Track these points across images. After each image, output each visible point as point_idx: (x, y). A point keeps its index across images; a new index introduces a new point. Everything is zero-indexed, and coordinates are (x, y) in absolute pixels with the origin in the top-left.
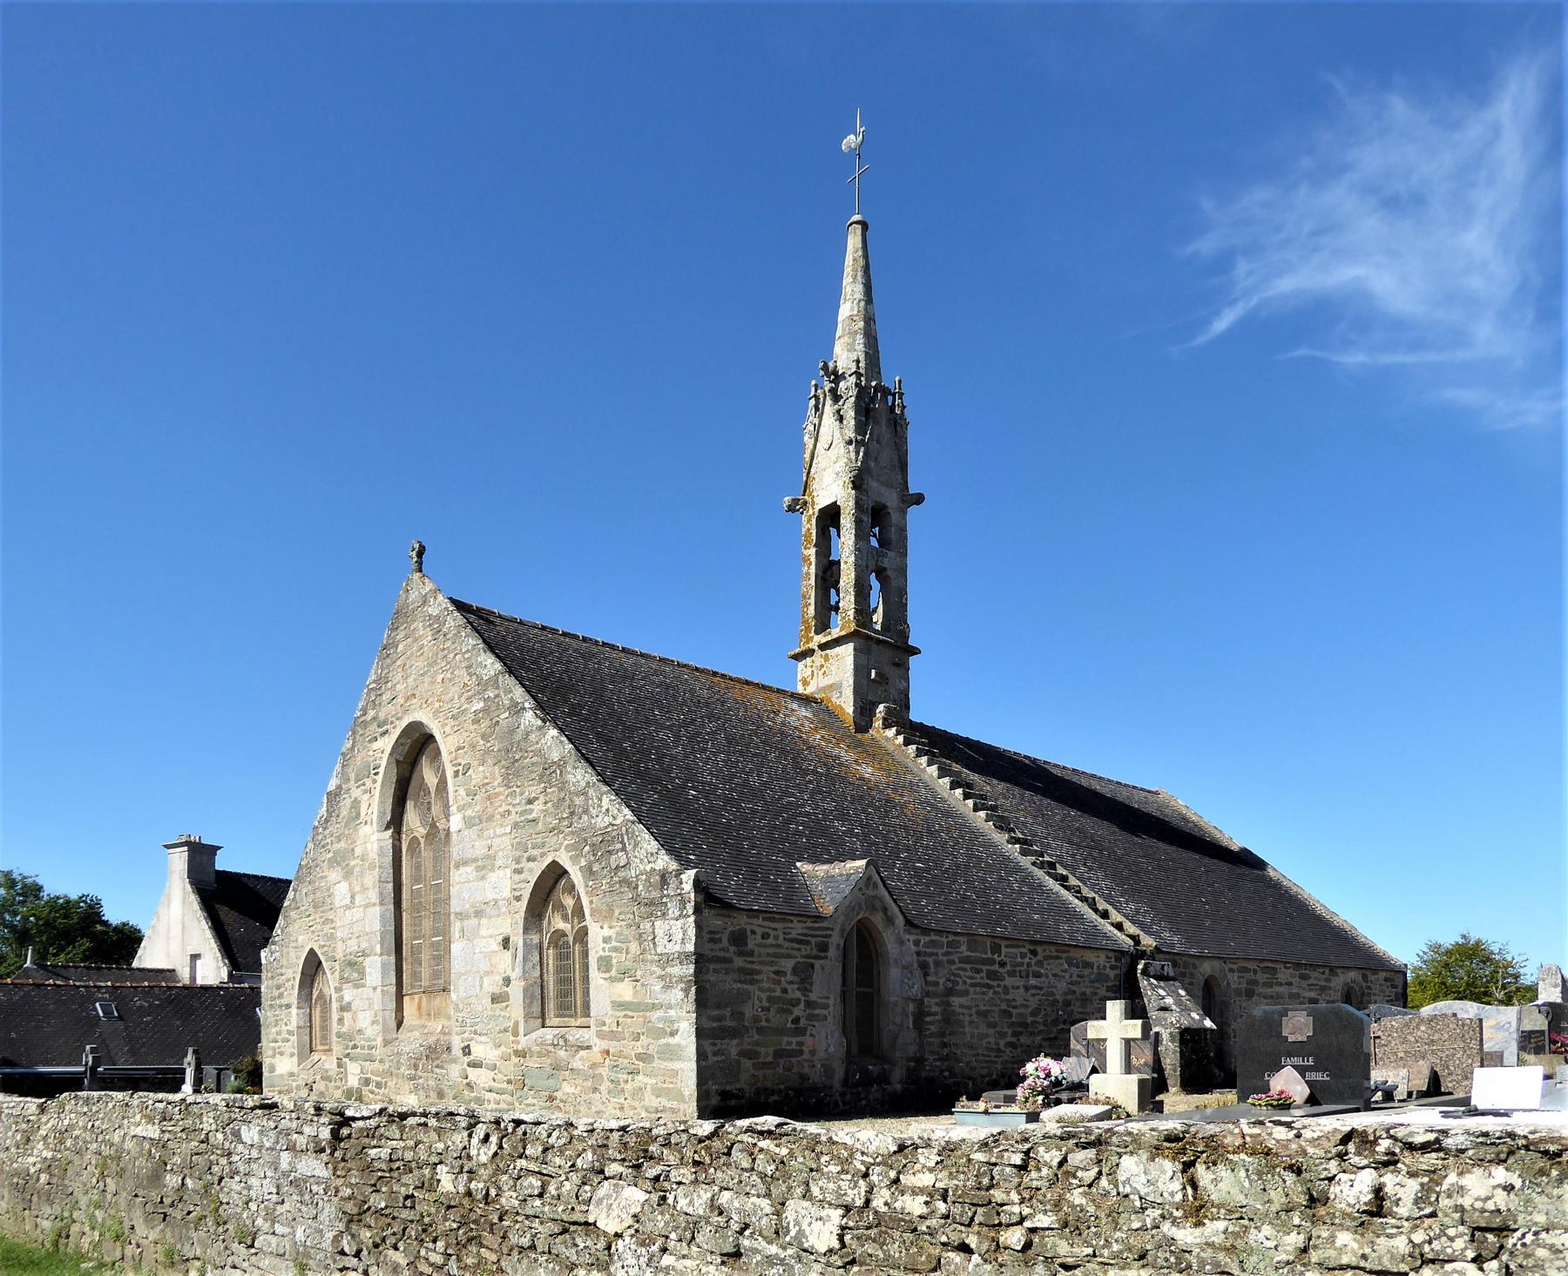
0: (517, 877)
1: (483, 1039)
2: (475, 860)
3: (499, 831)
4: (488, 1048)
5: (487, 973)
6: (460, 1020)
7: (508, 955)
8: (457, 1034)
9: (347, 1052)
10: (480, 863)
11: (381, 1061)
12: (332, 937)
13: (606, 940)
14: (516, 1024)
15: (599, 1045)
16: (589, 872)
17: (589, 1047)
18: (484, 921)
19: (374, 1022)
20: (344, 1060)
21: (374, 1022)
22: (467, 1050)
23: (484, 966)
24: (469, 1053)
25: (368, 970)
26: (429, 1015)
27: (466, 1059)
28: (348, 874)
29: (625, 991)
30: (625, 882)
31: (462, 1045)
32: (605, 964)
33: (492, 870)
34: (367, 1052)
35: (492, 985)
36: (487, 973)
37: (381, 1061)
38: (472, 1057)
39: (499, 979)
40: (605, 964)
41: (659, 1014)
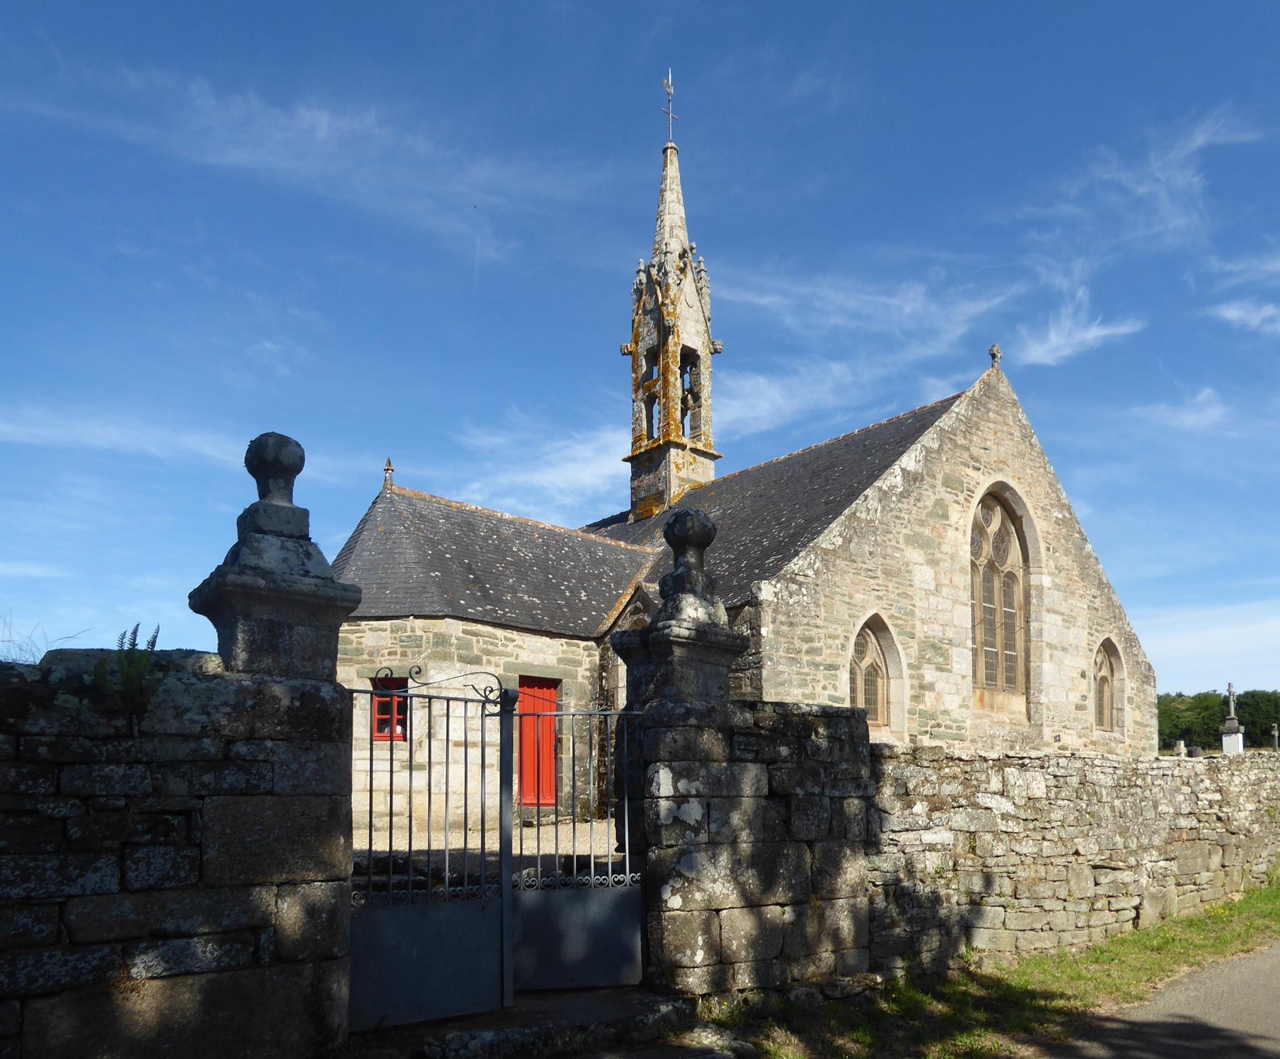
0: (1090, 637)
1: (1070, 731)
2: (1062, 614)
3: (1078, 604)
4: (1074, 738)
5: (1070, 690)
6: (1051, 717)
7: (1085, 682)
8: (1048, 726)
9: (924, 729)
10: (1066, 617)
11: (973, 741)
12: (912, 613)
13: (1132, 689)
14: (1091, 724)
15: (1128, 741)
16: (1125, 648)
17: (1124, 742)
18: (1068, 656)
19: (961, 706)
20: (919, 737)
21: (961, 706)
22: (1057, 739)
23: (1068, 684)
24: (1059, 740)
25: (955, 658)
26: (992, 707)
27: (1057, 744)
28: (933, 562)
29: (1138, 716)
30: (1138, 663)
31: (1054, 734)
32: (1130, 700)
33: (1074, 626)
34: (955, 732)
35: (1075, 698)
36: (1070, 690)
37: (973, 741)
38: (1061, 744)
39: (1079, 695)
40: (1130, 700)
41: (1148, 729)
